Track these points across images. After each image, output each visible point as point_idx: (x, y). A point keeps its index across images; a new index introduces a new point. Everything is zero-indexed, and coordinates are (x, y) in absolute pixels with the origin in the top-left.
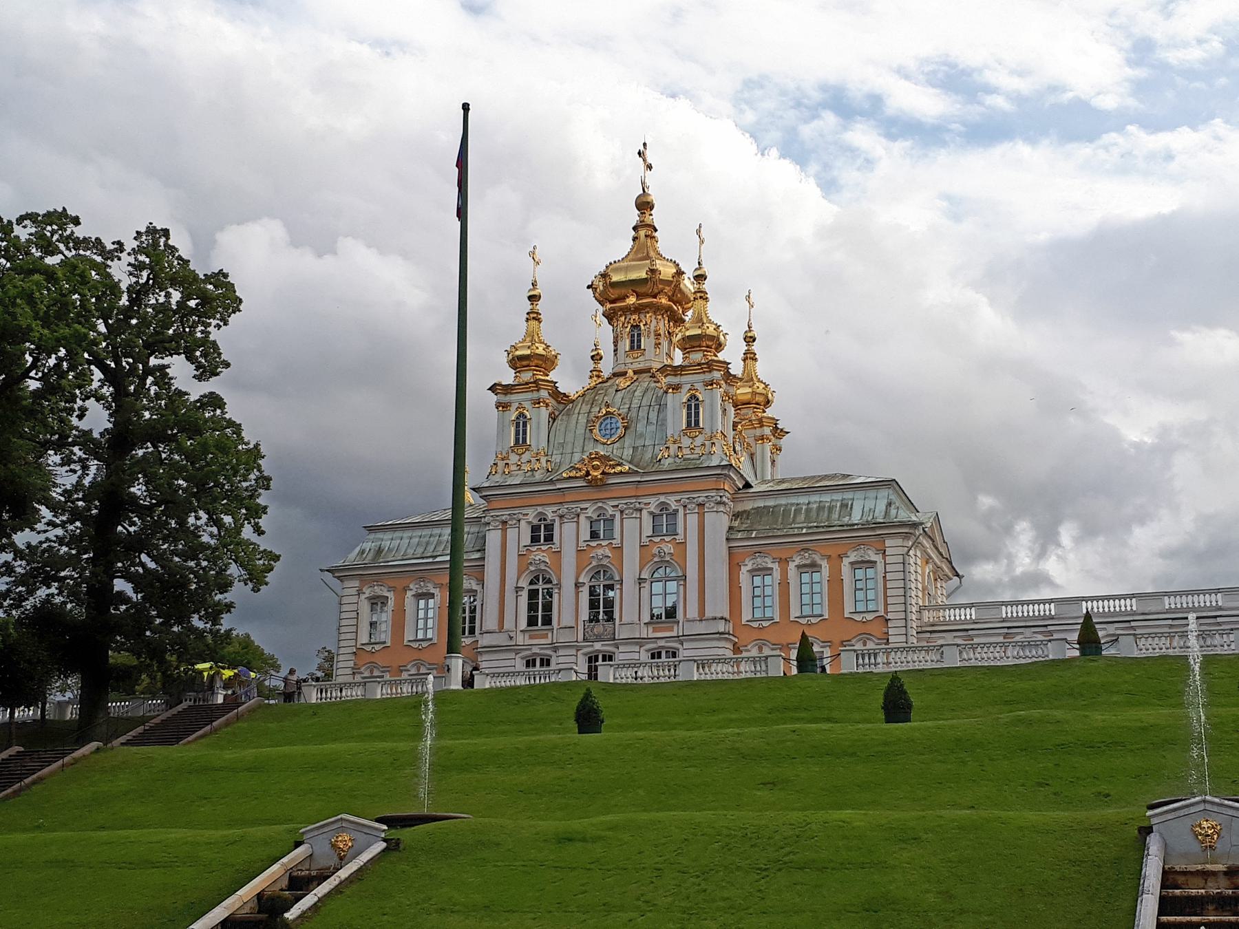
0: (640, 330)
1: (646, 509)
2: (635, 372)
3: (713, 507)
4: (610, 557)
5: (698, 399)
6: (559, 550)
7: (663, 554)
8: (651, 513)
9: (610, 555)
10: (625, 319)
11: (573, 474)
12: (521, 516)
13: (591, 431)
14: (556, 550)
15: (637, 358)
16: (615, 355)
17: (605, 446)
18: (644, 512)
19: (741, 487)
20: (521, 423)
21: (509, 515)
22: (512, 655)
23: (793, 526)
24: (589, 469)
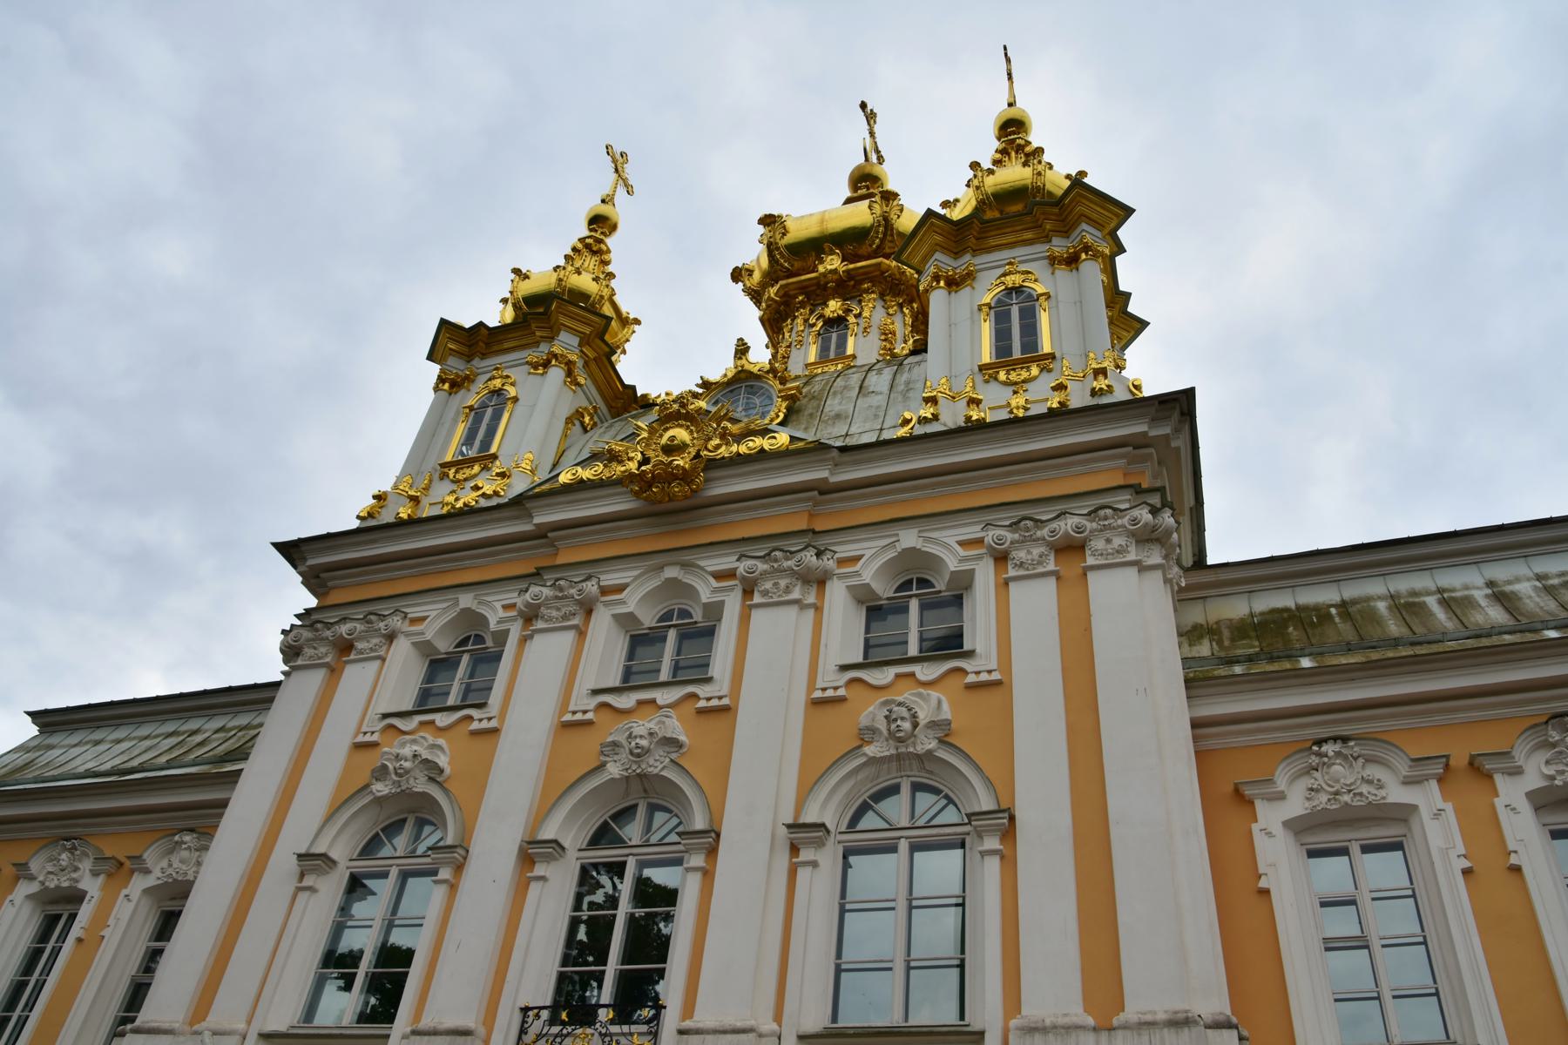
0: (847, 327)
1: (842, 577)
3: (1121, 551)
6: (493, 724)
7: (907, 725)
9: (683, 738)
14: (485, 725)
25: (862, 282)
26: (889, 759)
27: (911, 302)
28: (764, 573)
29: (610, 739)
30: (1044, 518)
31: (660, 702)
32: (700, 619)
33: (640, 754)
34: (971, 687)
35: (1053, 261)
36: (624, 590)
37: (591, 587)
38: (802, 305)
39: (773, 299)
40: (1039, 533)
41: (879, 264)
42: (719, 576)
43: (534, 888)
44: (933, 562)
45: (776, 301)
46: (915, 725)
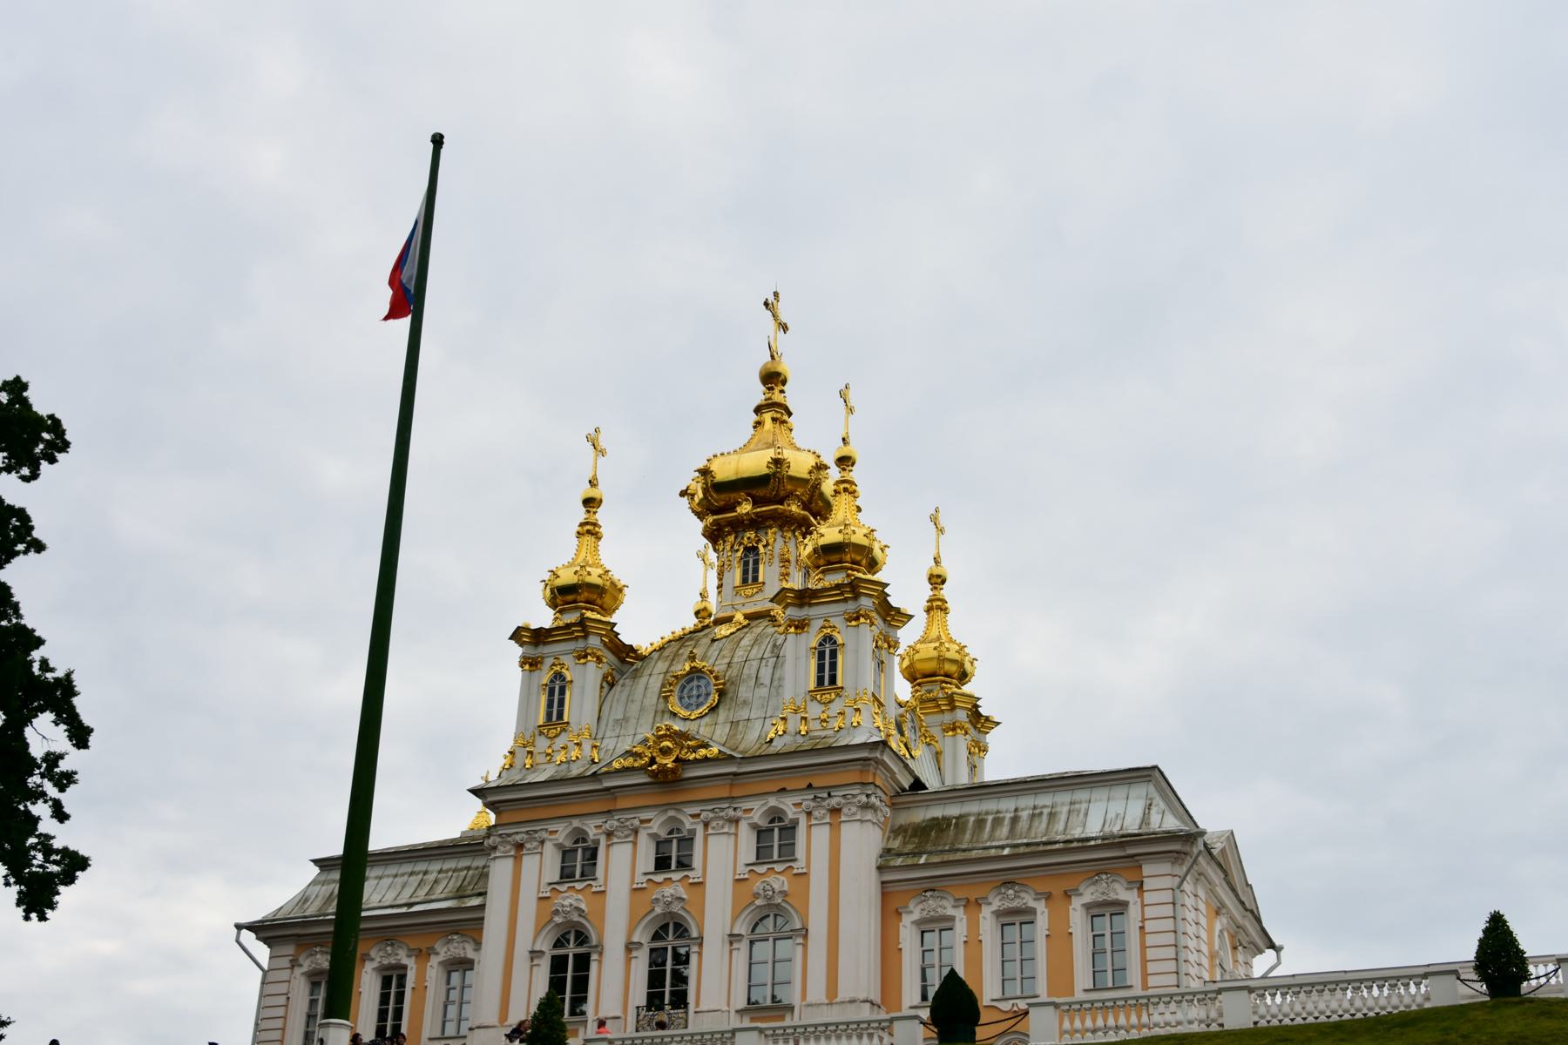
0: (758, 554)
1: (745, 819)
2: (747, 617)
4: (683, 900)
5: (835, 642)
6: (602, 889)
7: (770, 893)
8: (754, 826)
9: (684, 896)
10: (736, 538)
11: (629, 762)
12: (545, 835)
13: (666, 698)
14: (598, 889)
15: (752, 596)
16: (719, 593)
17: (688, 722)
18: (743, 826)
19: (907, 788)
20: (557, 690)
21: (527, 832)
23: (988, 844)
24: (654, 754)
26: (764, 906)
29: (654, 897)
31: (674, 879)
34: (796, 875)
37: (636, 822)
38: (729, 534)
41: (776, 509)
42: (693, 816)
43: (633, 961)
46: (774, 892)
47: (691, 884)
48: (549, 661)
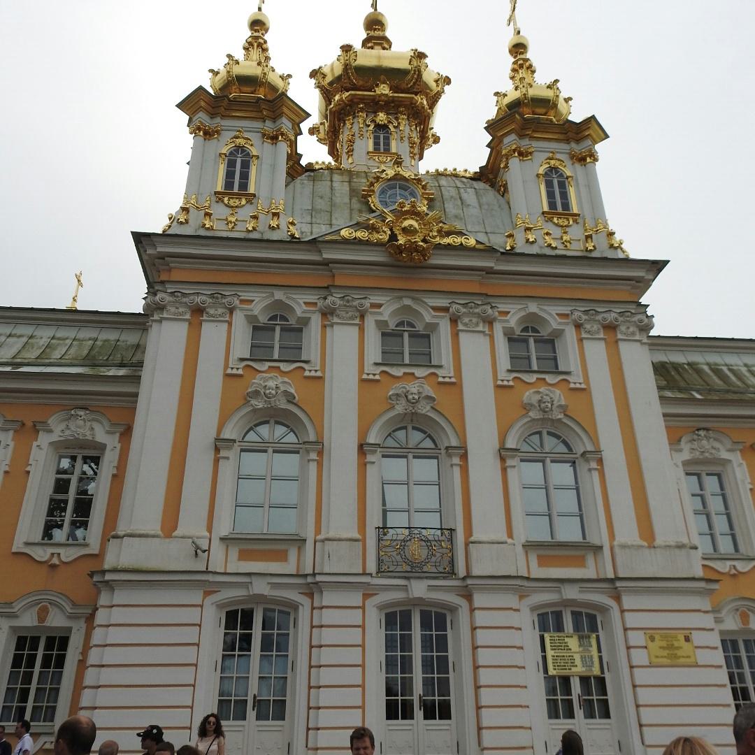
5: (561, 175)
6: (319, 374)
7: (550, 405)
14: (313, 374)
22: (196, 597)
25: (399, 106)
26: (538, 420)
27: (420, 124)
28: (464, 313)
30: (599, 310)
31: (417, 375)
32: (421, 330)
33: (414, 403)
35: (572, 157)
36: (381, 306)
38: (362, 110)
39: (343, 101)
40: (597, 318)
42: (435, 309)
44: (543, 321)
45: (345, 103)
47: (440, 383)
48: (227, 136)
